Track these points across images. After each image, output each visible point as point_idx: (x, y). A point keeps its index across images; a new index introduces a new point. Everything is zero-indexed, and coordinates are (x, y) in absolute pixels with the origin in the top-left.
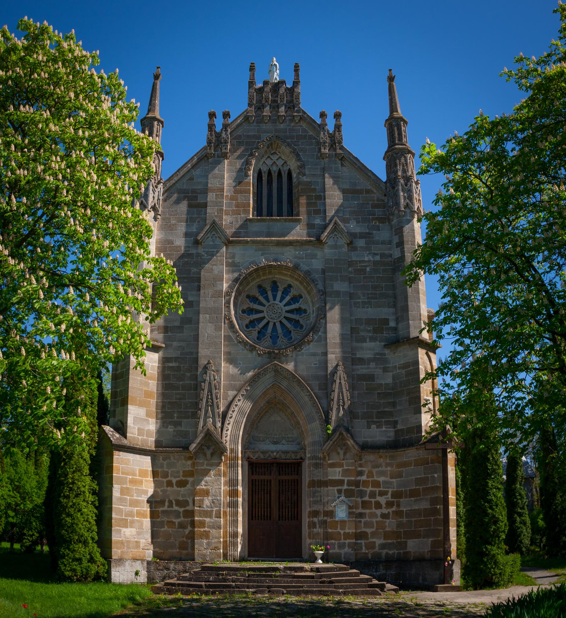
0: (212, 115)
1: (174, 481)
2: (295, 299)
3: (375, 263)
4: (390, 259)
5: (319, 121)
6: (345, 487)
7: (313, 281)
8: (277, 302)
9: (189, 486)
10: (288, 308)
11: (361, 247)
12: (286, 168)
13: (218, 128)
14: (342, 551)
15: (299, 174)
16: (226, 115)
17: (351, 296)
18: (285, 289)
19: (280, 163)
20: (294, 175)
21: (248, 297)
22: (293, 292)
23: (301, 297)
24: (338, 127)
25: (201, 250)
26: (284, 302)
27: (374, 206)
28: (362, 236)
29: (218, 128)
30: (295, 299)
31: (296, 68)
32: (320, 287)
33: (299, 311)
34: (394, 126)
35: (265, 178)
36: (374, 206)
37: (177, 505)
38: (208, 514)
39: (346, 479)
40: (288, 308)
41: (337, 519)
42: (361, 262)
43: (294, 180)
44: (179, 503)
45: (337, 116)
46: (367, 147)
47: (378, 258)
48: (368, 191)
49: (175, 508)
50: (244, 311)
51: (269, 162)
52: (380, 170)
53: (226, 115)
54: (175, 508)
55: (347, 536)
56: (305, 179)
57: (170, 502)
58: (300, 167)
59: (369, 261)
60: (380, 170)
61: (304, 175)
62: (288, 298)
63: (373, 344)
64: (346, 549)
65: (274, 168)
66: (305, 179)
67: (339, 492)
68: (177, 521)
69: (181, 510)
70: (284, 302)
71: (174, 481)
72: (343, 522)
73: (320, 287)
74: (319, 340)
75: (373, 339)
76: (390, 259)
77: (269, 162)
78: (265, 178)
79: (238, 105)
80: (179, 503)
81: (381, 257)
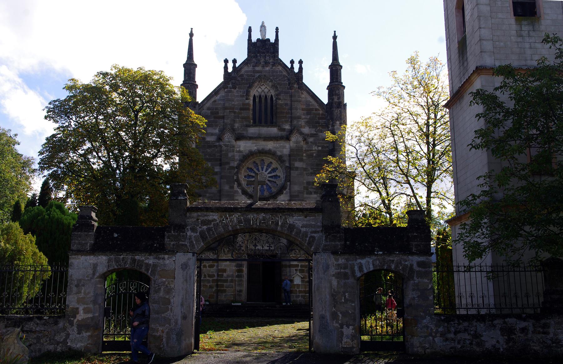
0: (226, 61)
1: (207, 265)
2: (274, 170)
3: (319, 151)
4: (327, 149)
5: (289, 66)
6: (300, 268)
7: (284, 161)
8: (264, 172)
9: (215, 268)
10: (270, 175)
11: (311, 142)
12: (269, 94)
13: (230, 70)
14: (298, 299)
15: (277, 99)
16: (234, 61)
17: (305, 169)
18: (268, 164)
19: (266, 90)
20: (274, 99)
21: (248, 168)
22: (274, 166)
23: (277, 169)
24: (301, 69)
25: (221, 143)
26: (268, 172)
27: (320, 118)
28: (312, 135)
29: (230, 70)
30: (274, 170)
31: (277, 29)
32: (287, 164)
33: (276, 177)
34: (335, 69)
35: (257, 100)
36: (320, 118)
37: (209, 277)
38: (226, 281)
39: (300, 264)
40: (270, 175)
41: (295, 283)
42: (311, 150)
43: (274, 102)
44: (209, 276)
45: (301, 62)
46: (317, 82)
47: (320, 148)
48: (316, 110)
49: (208, 278)
50: (245, 177)
51: (260, 90)
52: (324, 98)
53: (234, 61)
54: (208, 278)
55: (300, 292)
56: (280, 102)
57: (205, 276)
58: (277, 95)
59: (315, 150)
60: (324, 98)
61: (280, 99)
62: (270, 170)
63: (315, 196)
64: (300, 298)
65: (263, 94)
66: (280, 102)
67: (296, 270)
68: (208, 285)
69: (211, 279)
70: (268, 172)
71: (207, 265)
72: (298, 285)
73: (287, 164)
74: (286, 194)
75: (315, 193)
76: (327, 149)
77: (260, 90)
78: (257, 100)
79: (242, 56)
80: (209, 276)
81: (322, 148)
